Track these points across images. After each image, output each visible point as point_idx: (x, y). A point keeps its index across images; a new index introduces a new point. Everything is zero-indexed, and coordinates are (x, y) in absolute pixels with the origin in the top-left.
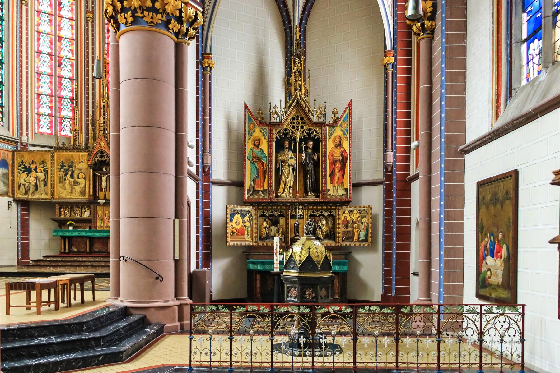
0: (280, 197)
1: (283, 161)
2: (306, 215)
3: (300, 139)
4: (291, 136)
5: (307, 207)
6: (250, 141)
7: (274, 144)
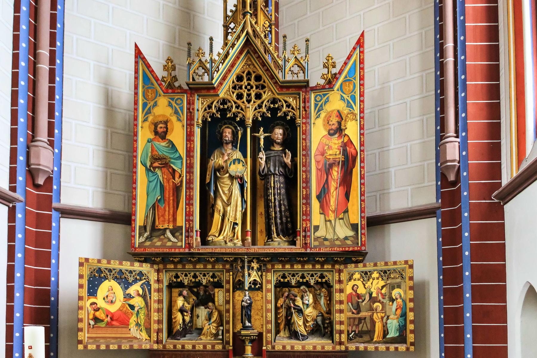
0: (213, 243)
1: (219, 169)
2: (269, 282)
4: (235, 115)
5: (269, 266)
6: (147, 124)
7: (197, 132)
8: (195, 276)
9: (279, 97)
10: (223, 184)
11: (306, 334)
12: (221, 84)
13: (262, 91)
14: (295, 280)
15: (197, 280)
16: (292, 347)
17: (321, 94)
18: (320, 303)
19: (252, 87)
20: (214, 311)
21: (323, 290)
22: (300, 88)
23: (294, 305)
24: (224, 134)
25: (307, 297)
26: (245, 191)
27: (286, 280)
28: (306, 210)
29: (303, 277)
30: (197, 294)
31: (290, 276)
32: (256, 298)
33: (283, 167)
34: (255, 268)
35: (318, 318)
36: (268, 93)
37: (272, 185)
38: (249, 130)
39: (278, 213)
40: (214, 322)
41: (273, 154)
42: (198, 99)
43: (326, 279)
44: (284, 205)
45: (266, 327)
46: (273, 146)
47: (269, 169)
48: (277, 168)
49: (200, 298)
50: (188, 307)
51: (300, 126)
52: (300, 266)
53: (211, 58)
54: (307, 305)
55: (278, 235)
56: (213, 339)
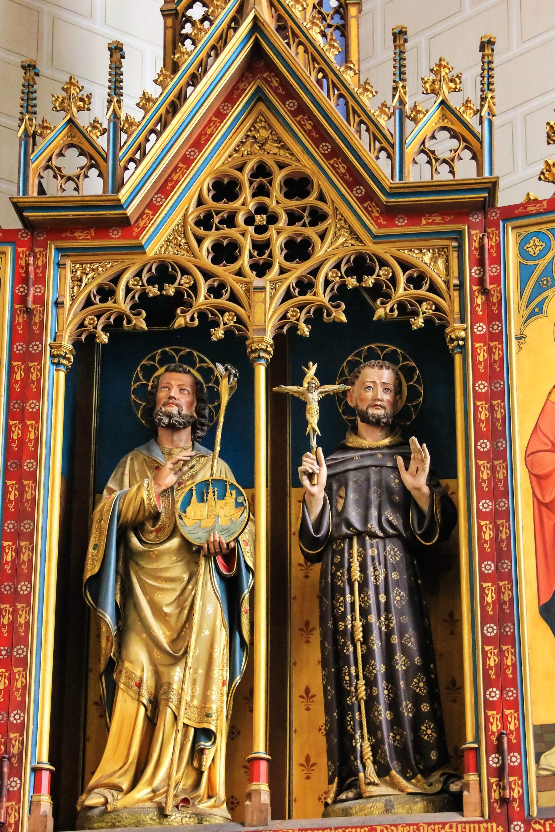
1: (135, 525)
3: (285, 339)
7: (55, 385)
9: (380, 250)
10: (157, 578)
12: (152, 207)
13: (312, 233)
17: (544, 228)
19: (273, 219)
22: (461, 211)
24: (162, 395)
26: (245, 605)
28: (500, 665)
33: (394, 505)
36: (336, 237)
37: (356, 574)
38: (261, 372)
39: (381, 683)
41: (355, 460)
42: (59, 265)
44: (405, 650)
46: (355, 431)
47: (341, 517)
48: (374, 513)
51: (463, 348)
53: (115, 115)
55: (383, 771)
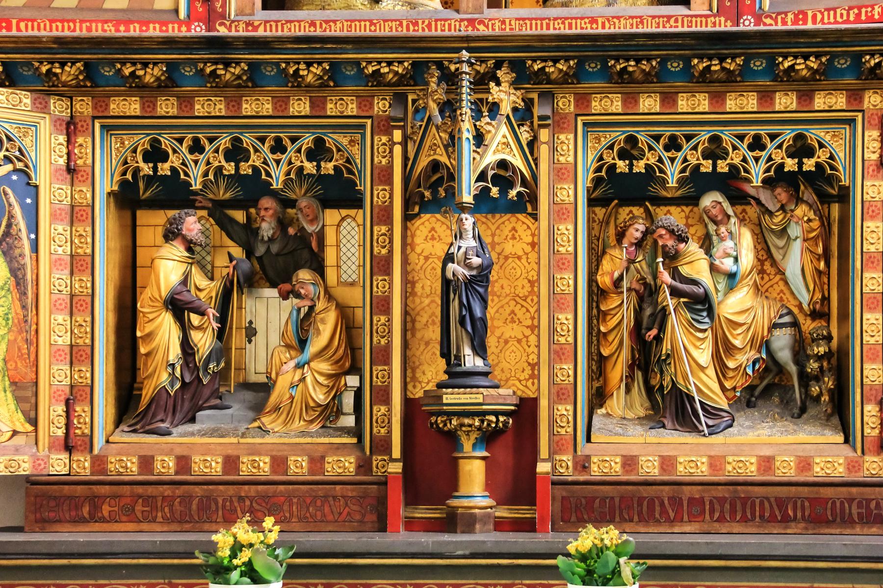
2: (561, 173)
5: (566, 103)
8: (236, 153)
11: (723, 404)
14: (678, 166)
15: (245, 169)
16: (667, 463)
18: (781, 272)
20: (320, 306)
21: (801, 210)
23: (675, 274)
25: (729, 244)
27: (640, 167)
29: (716, 149)
30: (246, 236)
31: (659, 147)
32: (509, 248)
34: (506, 108)
35: (777, 332)
40: (319, 355)
43: (822, 156)
45: (552, 375)
49: (260, 250)
50: (206, 289)
52: (702, 102)
54: (732, 276)
56: (315, 427)
